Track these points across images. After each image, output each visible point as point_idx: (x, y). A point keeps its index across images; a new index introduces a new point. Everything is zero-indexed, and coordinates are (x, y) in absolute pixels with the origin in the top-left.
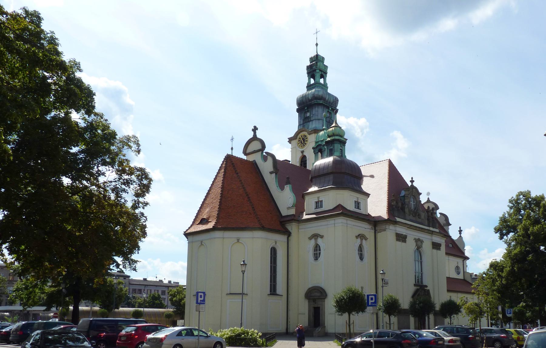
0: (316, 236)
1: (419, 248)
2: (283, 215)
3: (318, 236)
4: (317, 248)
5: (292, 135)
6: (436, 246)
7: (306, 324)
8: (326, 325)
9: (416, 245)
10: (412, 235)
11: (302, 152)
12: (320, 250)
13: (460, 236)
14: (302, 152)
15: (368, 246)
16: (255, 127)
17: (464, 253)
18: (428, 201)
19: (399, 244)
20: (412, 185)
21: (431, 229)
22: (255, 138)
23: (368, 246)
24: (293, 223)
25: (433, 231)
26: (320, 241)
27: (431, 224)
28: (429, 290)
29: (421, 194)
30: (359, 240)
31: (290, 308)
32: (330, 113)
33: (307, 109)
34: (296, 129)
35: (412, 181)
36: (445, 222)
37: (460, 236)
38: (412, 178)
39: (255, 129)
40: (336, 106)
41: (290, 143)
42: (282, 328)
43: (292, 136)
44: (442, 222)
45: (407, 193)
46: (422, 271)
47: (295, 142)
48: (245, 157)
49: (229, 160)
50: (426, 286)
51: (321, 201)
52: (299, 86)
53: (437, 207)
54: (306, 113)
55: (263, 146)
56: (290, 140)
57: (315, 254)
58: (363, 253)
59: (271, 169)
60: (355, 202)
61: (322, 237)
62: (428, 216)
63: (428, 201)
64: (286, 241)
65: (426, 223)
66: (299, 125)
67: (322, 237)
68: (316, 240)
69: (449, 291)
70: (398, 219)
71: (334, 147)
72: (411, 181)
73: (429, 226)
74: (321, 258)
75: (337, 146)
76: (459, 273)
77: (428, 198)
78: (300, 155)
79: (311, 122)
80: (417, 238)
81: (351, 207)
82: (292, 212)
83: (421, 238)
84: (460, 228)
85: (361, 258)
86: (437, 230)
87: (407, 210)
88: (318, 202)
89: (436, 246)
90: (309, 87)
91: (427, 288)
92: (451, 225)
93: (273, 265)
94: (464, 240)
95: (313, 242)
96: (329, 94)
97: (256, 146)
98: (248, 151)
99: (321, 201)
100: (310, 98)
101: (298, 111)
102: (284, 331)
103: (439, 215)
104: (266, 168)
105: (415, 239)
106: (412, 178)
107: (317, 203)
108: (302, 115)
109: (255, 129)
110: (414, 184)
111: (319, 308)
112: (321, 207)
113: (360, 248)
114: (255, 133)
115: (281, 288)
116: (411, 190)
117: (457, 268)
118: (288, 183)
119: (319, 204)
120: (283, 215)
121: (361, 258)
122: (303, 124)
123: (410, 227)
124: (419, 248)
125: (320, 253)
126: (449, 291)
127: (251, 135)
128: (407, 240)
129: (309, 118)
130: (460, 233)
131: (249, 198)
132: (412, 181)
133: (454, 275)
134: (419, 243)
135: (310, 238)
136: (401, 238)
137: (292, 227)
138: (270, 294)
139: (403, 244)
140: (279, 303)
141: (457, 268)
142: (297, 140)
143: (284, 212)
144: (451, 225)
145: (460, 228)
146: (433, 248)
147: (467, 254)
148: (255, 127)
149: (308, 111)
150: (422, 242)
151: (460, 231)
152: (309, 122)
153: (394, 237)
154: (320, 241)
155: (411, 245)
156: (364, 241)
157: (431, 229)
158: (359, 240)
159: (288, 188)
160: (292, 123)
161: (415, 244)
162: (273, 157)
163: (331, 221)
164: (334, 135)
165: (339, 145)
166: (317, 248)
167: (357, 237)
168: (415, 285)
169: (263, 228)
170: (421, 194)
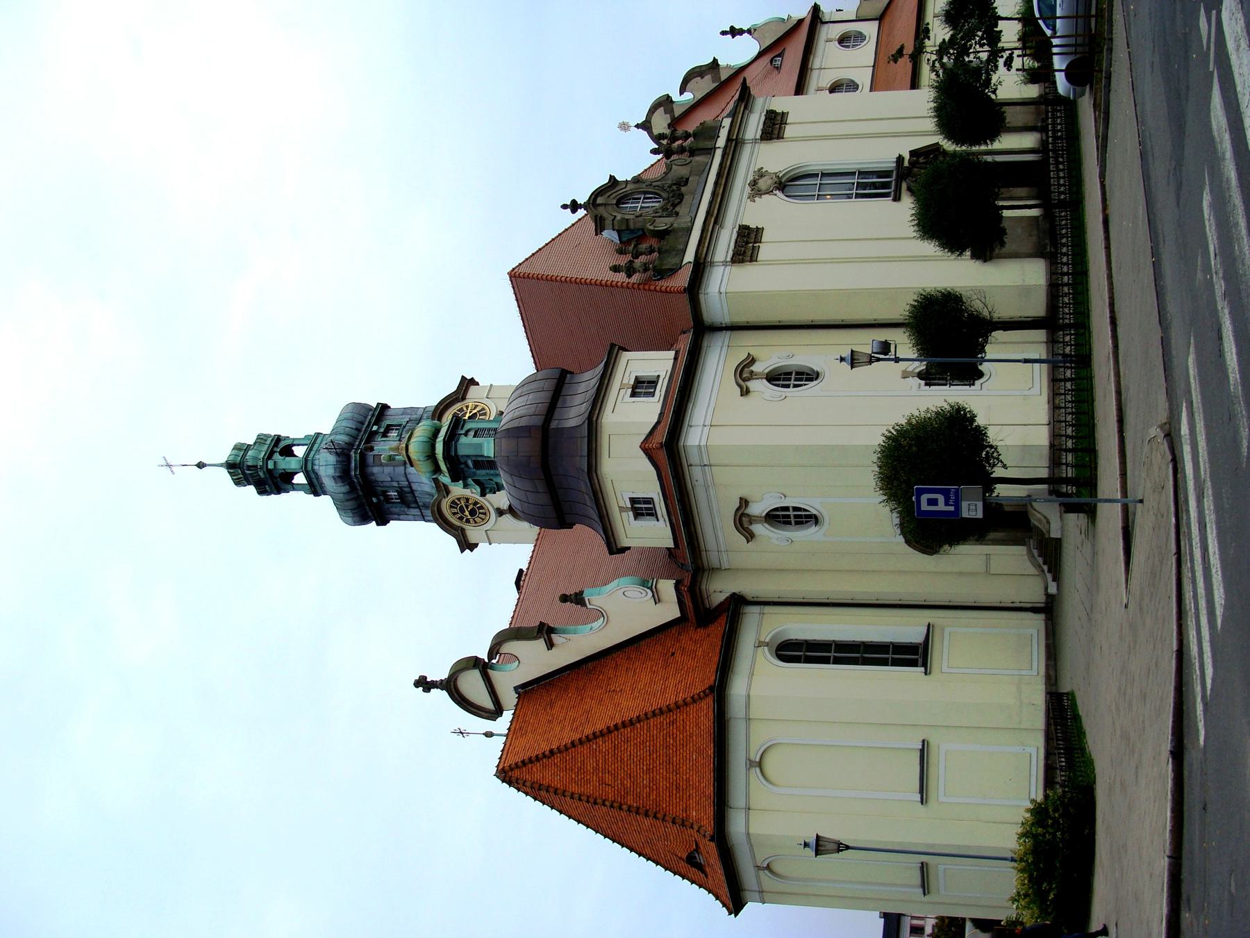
0: (743, 521)
2: (678, 614)
3: (743, 514)
4: (779, 517)
5: (452, 541)
7: (1020, 550)
9: (769, 192)
12: (787, 509)
13: (749, 31)
15: (774, 352)
17: (800, 22)
18: (645, 126)
19: (765, 251)
20: (585, 206)
21: (721, 142)
22: (450, 686)
23: (774, 352)
24: (703, 587)
25: (729, 140)
26: (758, 508)
27: (708, 144)
28: (913, 153)
29: (612, 178)
30: (753, 385)
31: (969, 601)
32: (389, 428)
33: (377, 496)
34: (434, 527)
35: (574, 206)
36: (708, 78)
37: (749, 31)
38: (564, 207)
39: (424, 684)
40: (366, 408)
41: (476, 545)
42: (1035, 624)
43: (454, 540)
44: (705, 85)
45: (608, 222)
46: (854, 173)
47: (473, 533)
48: (507, 716)
49: (511, 773)
50: (900, 159)
51: (633, 501)
52: (311, 515)
53: (665, 103)
54: (388, 499)
55: (475, 663)
56: (466, 545)
57: (797, 523)
58: (793, 369)
59: (540, 644)
60: (633, 395)
61: (744, 502)
62: (682, 150)
63: (645, 126)
64: (756, 609)
65: (699, 159)
66: (424, 519)
67: (744, 502)
68: (752, 519)
69: (915, 84)
70: (690, 256)
71: (468, 456)
72: (574, 211)
73: (711, 151)
74: (811, 503)
75: (466, 444)
76: (860, 37)
77: (638, 126)
78: (507, 518)
79: (414, 487)
80: (748, 189)
81: (648, 411)
82: (667, 587)
83: (750, 178)
84: (724, 33)
85: (807, 376)
86: (727, 122)
87: (662, 224)
88: (634, 509)
89: (774, 126)
90: (315, 488)
91: (907, 157)
92: (715, 60)
93: (832, 654)
94: (759, 20)
95: (759, 529)
96: (334, 432)
97: (472, 685)
98: (488, 703)
99: (633, 501)
100: (345, 489)
101: (382, 521)
102: (1040, 618)
103: (688, 96)
104: (534, 660)
105: (752, 197)
106: (564, 207)
107: (638, 514)
108: (394, 510)
109: (424, 684)
110: (581, 201)
112: (649, 501)
113: (778, 378)
115: (906, 629)
116: (601, 210)
117: (843, 40)
118: (578, 599)
119: (641, 508)
120: (678, 614)
121: (807, 376)
122: (418, 507)
123: (715, 216)
125: (795, 509)
126: (915, 84)
127: (440, 695)
128: (753, 226)
129: (401, 492)
130: (741, 32)
131: (624, 725)
132: (574, 206)
133: (865, 54)
134: (763, 184)
135: (750, 536)
136: (748, 245)
137: (719, 590)
138: (925, 665)
139: (766, 237)
140: (959, 642)
141: (843, 40)
142: (466, 526)
143: (669, 611)
144: (715, 60)
145: (724, 33)
146: (780, 137)
147: (803, 12)
149: (384, 493)
150: (761, 174)
151: (734, 32)
152: (412, 491)
154: (758, 508)
155: (767, 213)
156: (756, 368)
157: (721, 142)
158: (753, 385)
159: (595, 598)
160: (415, 540)
162: (500, 640)
163: (696, 476)
164: (432, 456)
165: (463, 440)
166: (779, 517)
167: (745, 392)
168: (897, 198)
169: (719, 692)
170: (612, 178)
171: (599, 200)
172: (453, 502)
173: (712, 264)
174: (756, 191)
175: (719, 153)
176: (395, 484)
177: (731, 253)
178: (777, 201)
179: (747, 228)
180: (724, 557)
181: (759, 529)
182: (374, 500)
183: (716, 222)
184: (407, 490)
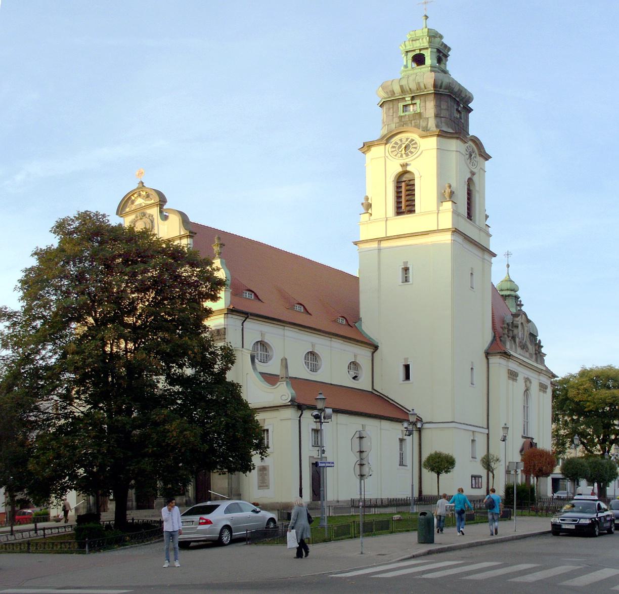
1: (527, 390)
6: (543, 387)
9: (526, 386)
10: (523, 373)
73: (536, 361)
80: (526, 377)
83: (530, 378)
86: (544, 368)
123: (523, 364)
124: (527, 390)
128: (518, 378)
136: (513, 375)
150: (530, 382)
153: (505, 375)
155: (520, 384)
161: (524, 384)
171: (523, 316)
173: (508, 361)
174: (527, 380)
175: (535, 364)
177: (511, 369)
178: (524, 389)
179: (517, 376)
183: (520, 364)
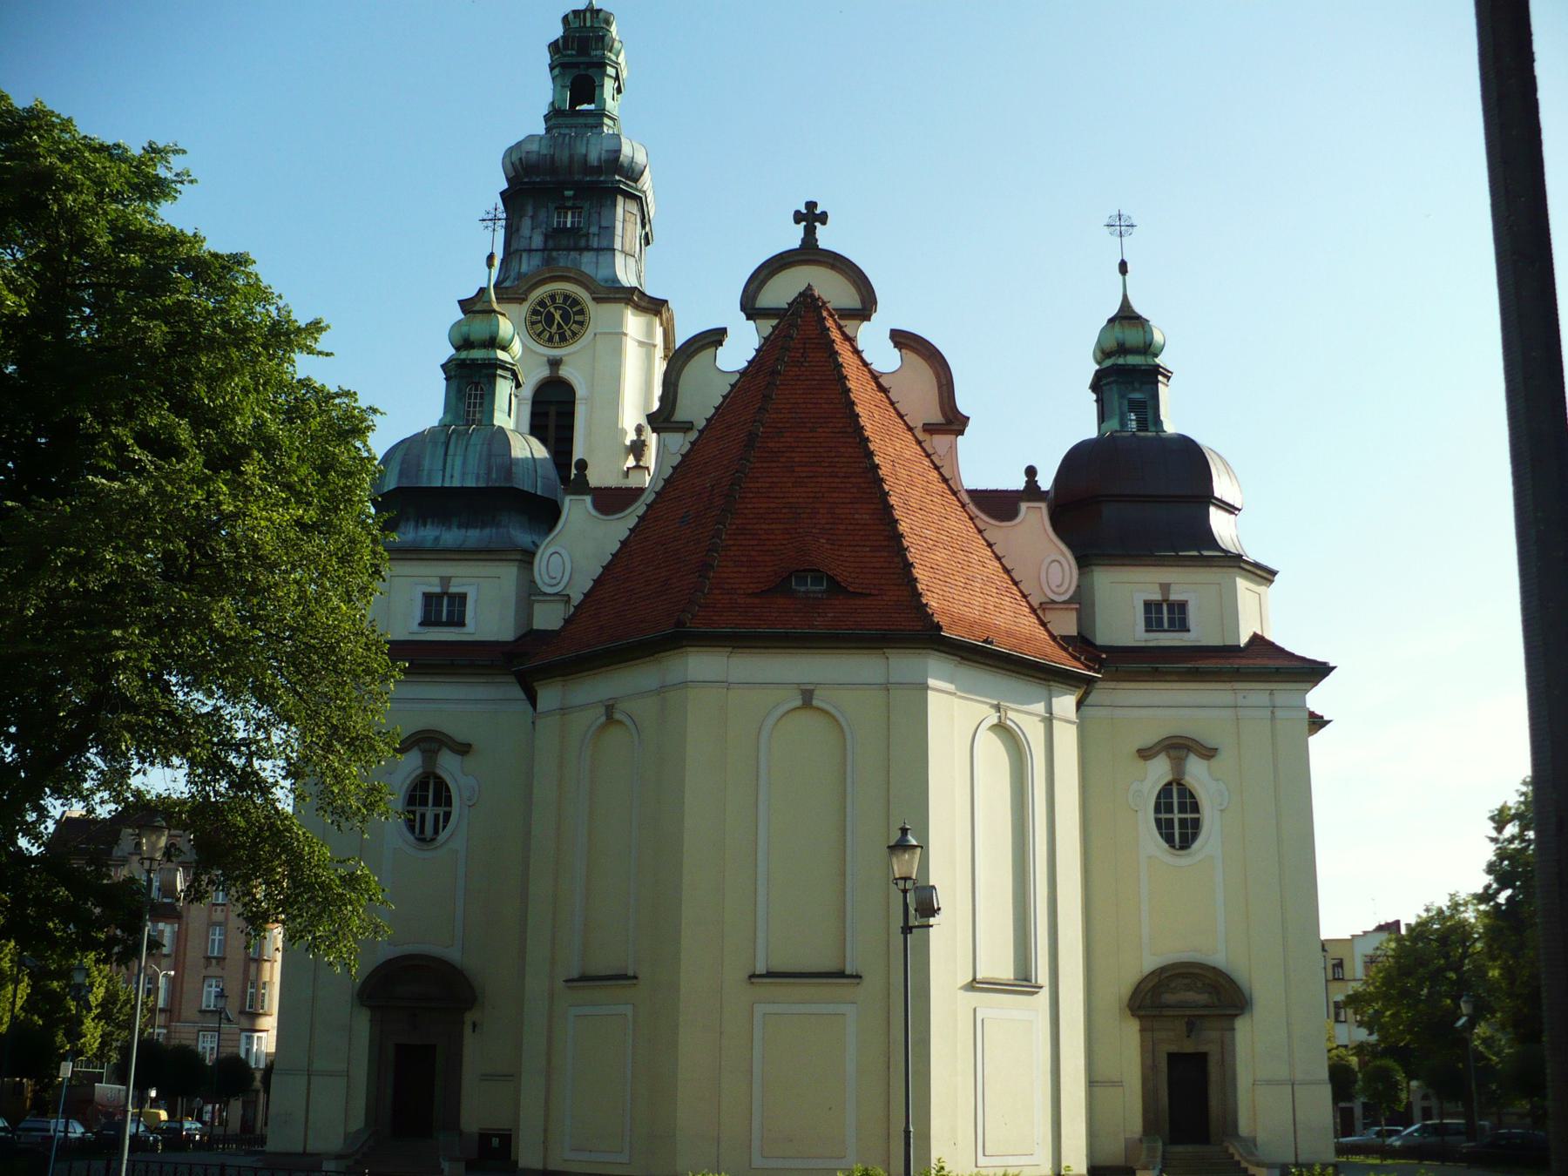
0: (1178, 747)
8: (1244, 1128)
11: (555, 363)
14: (555, 363)
16: (811, 205)
22: (809, 253)
26: (1197, 772)
33: (574, 197)
39: (811, 217)
51: (1182, 606)
61: (1209, 753)
99: (1182, 606)
111: (1202, 1058)
112: (1184, 627)
114: (810, 232)
127: (793, 237)
135: (1145, 754)
148: (811, 205)
154: (1197, 772)
172: (576, 302)
176: (594, 229)
180: (1103, 712)
181: (1159, 771)
182: (569, 193)
184: (583, 243)
